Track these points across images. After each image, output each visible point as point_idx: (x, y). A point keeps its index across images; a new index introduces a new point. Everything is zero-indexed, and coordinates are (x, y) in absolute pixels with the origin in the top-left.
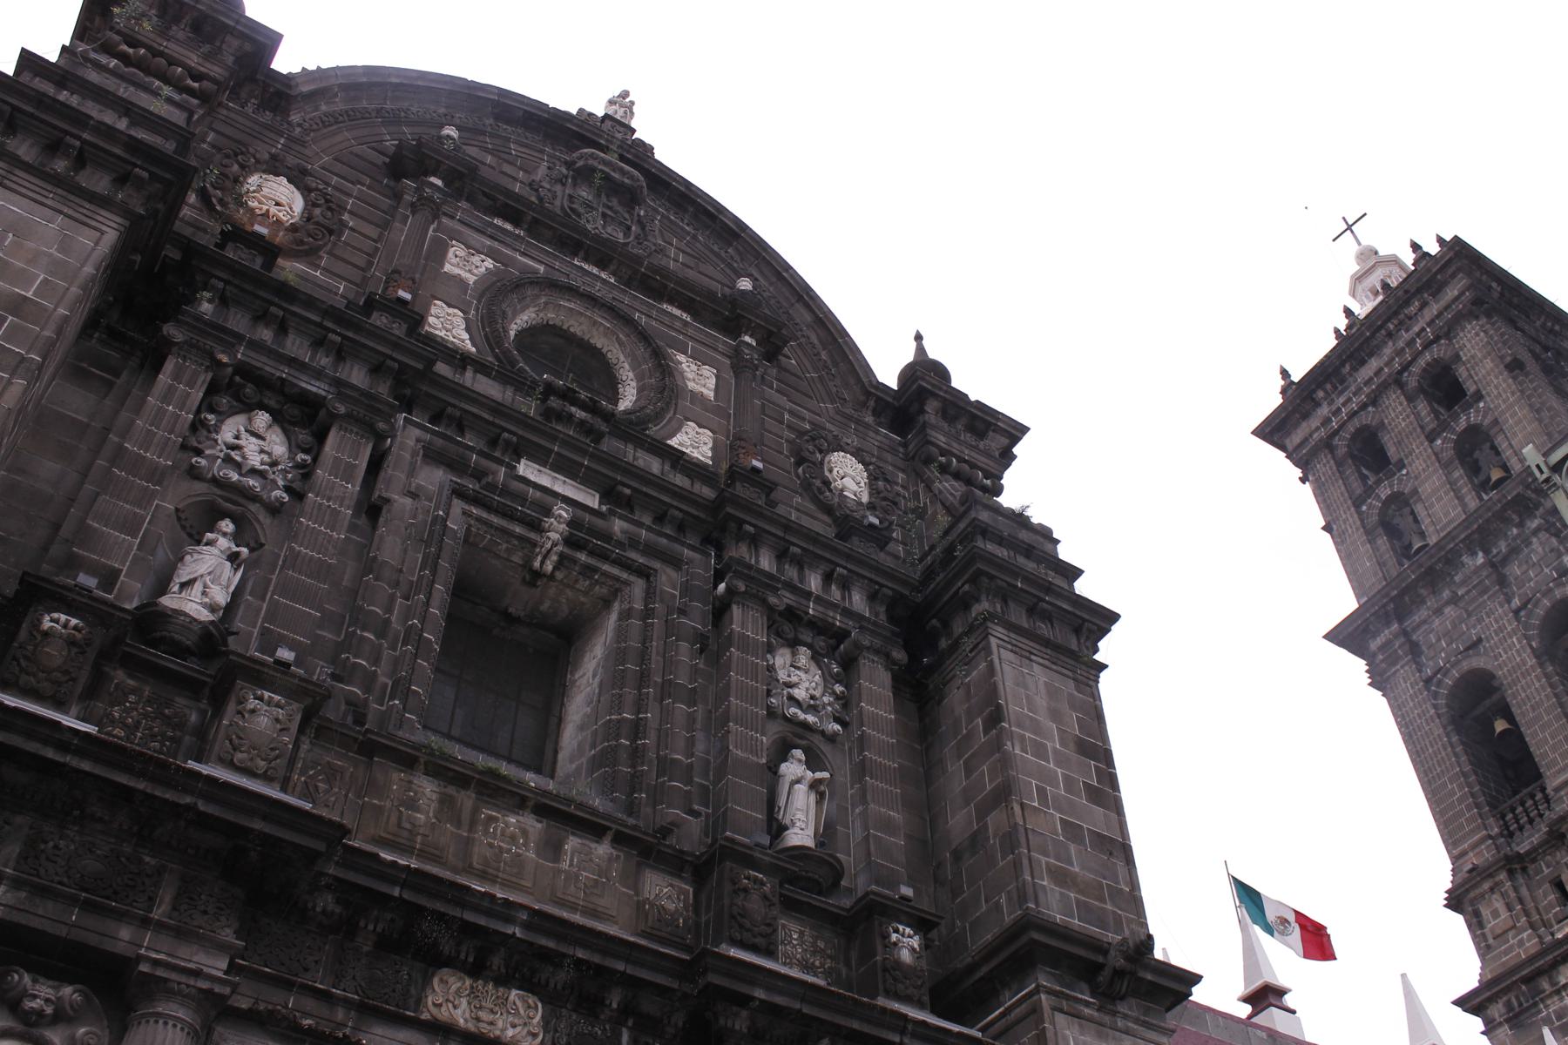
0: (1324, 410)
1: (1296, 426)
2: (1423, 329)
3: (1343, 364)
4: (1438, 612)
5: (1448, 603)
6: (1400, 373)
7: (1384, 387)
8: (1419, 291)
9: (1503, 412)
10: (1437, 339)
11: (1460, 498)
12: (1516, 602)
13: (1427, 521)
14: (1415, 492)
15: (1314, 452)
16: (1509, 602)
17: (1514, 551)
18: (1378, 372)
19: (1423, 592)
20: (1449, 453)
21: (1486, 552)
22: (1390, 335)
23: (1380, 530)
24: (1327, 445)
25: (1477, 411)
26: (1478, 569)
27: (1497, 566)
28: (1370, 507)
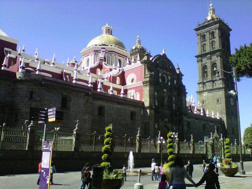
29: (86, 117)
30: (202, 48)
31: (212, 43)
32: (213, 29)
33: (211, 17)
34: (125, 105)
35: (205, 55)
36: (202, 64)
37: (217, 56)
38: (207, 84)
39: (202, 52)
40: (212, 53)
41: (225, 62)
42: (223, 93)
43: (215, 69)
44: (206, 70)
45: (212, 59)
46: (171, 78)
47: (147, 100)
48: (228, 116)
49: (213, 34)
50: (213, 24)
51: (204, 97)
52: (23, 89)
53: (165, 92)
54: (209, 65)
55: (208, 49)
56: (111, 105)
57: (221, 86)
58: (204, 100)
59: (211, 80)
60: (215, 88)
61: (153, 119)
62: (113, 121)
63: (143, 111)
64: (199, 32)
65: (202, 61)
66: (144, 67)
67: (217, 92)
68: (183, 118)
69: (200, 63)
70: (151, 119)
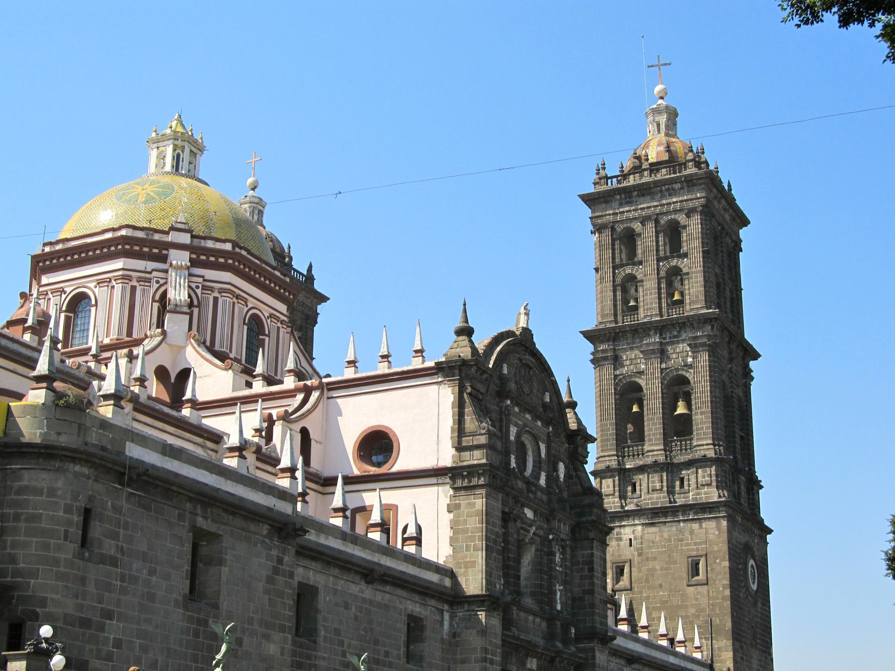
12: (663, 366)
21: (661, 335)
22: (661, 191)
29: (272, 649)
30: (619, 293)
31: (672, 279)
32: (676, 211)
33: (662, 148)
34: (388, 588)
35: (640, 331)
36: (616, 376)
37: (695, 348)
38: (642, 480)
39: (620, 318)
40: (669, 328)
41: (724, 377)
42: (719, 528)
43: (681, 409)
44: (635, 409)
45: (669, 358)
46: (548, 449)
47: (473, 563)
48: (737, 644)
49: (673, 232)
50: (677, 186)
51: (622, 543)
52: (52, 492)
53: (531, 523)
54: (652, 389)
55: (649, 305)
56: (341, 585)
57: (713, 495)
58: (623, 558)
59: (661, 459)
60: (680, 501)
61: (498, 659)
63: (452, 618)
64: (609, 214)
65: (616, 361)
67: (689, 525)
68: (594, 657)
69: (608, 370)
70: (492, 662)
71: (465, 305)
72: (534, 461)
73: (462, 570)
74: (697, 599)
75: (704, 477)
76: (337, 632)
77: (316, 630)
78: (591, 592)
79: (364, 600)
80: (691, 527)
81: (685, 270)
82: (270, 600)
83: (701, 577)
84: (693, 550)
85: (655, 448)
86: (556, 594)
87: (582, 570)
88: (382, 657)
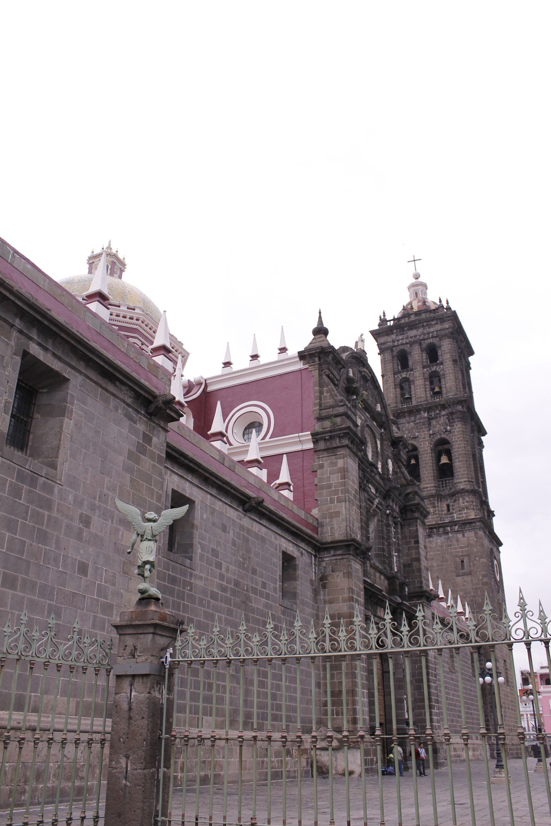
0: (394, 337)
1: (384, 336)
2: (434, 332)
3: (406, 327)
4: (409, 422)
5: (412, 422)
6: (422, 340)
7: (415, 342)
8: (437, 319)
9: (447, 374)
10: (437, 337)
11: (426, 391)
12: (431, 432)
13: (414, 392)
14: (414, 381)
15: (386, 349)
16: (429, 430)
17: (435, 418)
18: (415, 336)
19: (406, 415)
20: (427, 375)
21: (428, 413)
22: (423, 326)
23: (398, 386)
24: (391, 349)
25: (440, 368)
26: (424, 418)
27: (430, 419)
28: (398, 377)
31: (434, 378)
34: (264, 522)
43: (444, 460)
56: (218, 505)
62: (224, 589)
66: (316, 373)
70: (357, 601)
71: (320, 313)
72: (373, 452)
73: (328, 520)
74: (464, 585)
75: (463, 503)
76: (215, 553)
77: (191, 545)
78: (418, 560)
79: (242, 527)
80: (457, 537)
81: (441, 373)
82: (132, 480)
83: (466, 570)
84: (459, 552)
85: (429, 486)
86: (393, 558)
87: (409, 542)
88: (259, 588)
